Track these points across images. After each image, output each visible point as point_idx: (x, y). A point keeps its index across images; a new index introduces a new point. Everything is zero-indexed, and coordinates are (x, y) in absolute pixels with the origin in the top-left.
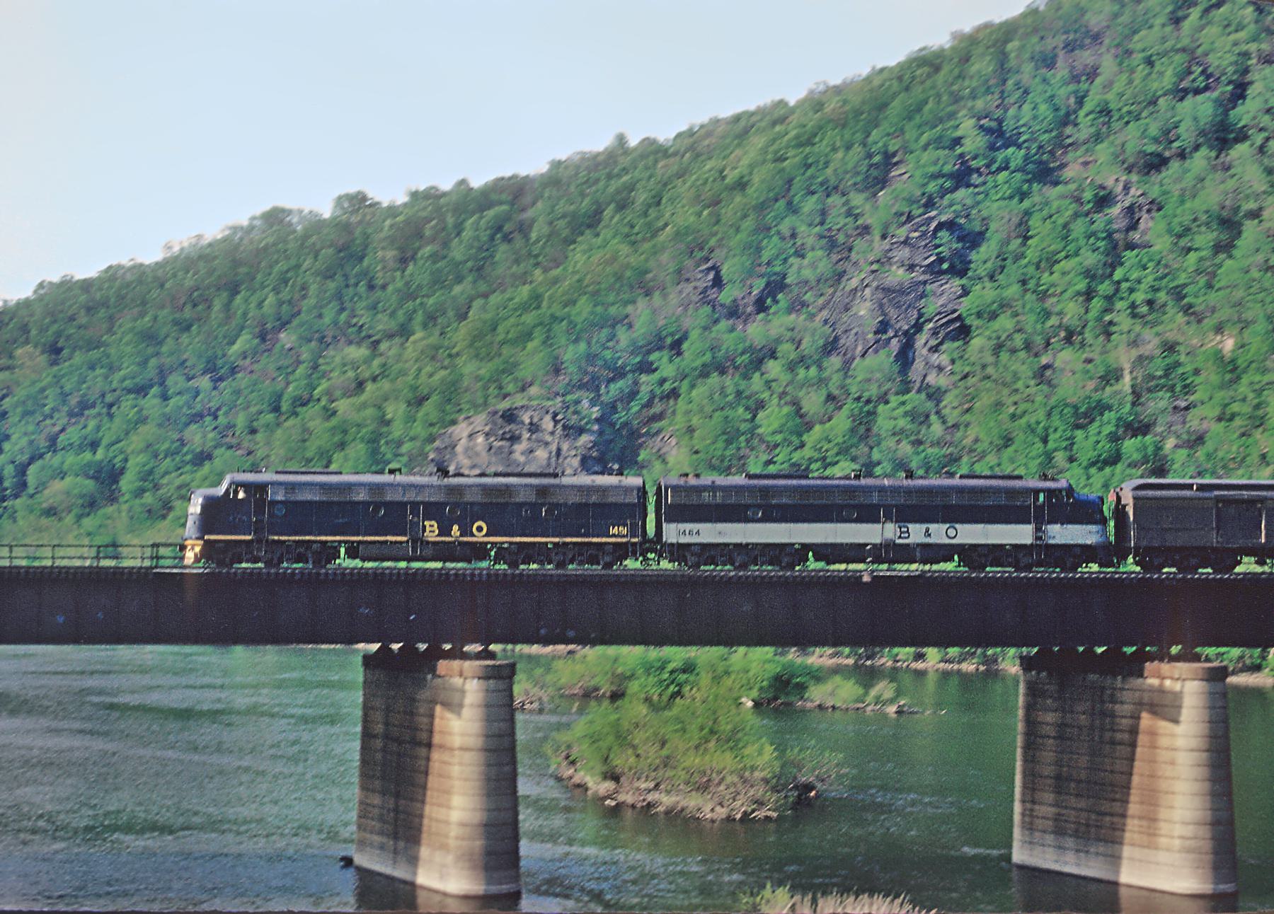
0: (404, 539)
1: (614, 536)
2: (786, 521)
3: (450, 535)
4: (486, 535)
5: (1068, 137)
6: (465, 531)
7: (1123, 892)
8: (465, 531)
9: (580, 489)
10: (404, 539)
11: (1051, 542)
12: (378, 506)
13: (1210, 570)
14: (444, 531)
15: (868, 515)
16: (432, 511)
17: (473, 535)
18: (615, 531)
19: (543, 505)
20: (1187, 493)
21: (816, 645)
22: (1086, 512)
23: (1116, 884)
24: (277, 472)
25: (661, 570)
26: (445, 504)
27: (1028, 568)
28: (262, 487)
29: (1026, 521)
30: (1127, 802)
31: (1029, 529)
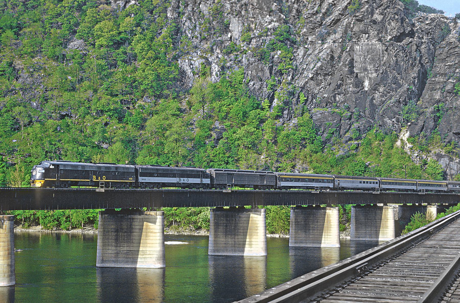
0: (89, 180)
1: (130, 180)
2: (162, 177)
3: (98, 179)
4: (105, 180)
5: (268, 106)
6: (101, 179)
7: (138, 271)
8: (101, 179)
9: (123, 168)
10: (89, 180)
11: (203, 183)
12: (83, 171)
13: (214, 189)
14: (97, 179)
15: (174, 176)
16: (95, 173)
17: (103, 180)
18: (130, 179)
19: (117, 172)
20: (222, 172)
21: (17, 210)
22: (204, 175)
23: (320, 247)
24: (151, 165)
25: (31, 188)
26: (97, 171)
27: (199, 188)
28: (58, 165)
29: (199, 178)
30: (246, 238)
31: (199, 179)
